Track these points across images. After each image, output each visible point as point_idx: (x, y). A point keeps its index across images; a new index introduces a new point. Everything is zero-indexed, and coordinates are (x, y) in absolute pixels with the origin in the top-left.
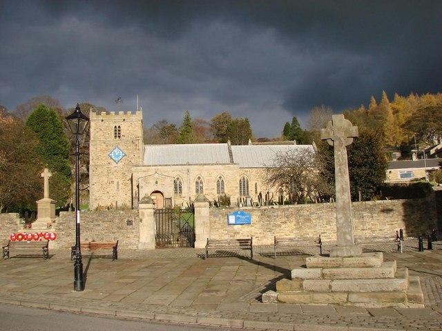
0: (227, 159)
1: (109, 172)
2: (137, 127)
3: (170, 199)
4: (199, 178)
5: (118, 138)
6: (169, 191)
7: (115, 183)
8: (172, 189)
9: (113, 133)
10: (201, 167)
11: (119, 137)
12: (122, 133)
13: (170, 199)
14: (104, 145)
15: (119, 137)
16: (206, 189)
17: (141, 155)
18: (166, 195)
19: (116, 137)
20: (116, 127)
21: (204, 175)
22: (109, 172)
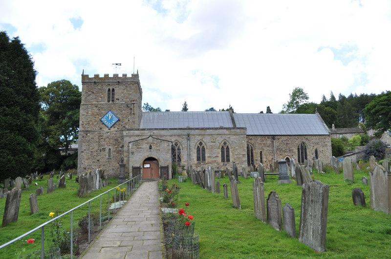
0: (231, 126)
1: (100, 136)
2: (133, 91)
3: (167, 167)
4: (201, 144)
5: (111, 102)
6: (165, 158)
7: (107, 150)
9: (106, 98)
10: (202, 132)
11: (113, 101)
12: (116, 97)
13: (167, 167)
14: (96, 110)
15: (113, 101)
16: (209, 157)
17: (137, 120)
18: (162, 163)
19: (109, 101)
20: (109, 90)
21: (207, 140)
22: (100, 136)
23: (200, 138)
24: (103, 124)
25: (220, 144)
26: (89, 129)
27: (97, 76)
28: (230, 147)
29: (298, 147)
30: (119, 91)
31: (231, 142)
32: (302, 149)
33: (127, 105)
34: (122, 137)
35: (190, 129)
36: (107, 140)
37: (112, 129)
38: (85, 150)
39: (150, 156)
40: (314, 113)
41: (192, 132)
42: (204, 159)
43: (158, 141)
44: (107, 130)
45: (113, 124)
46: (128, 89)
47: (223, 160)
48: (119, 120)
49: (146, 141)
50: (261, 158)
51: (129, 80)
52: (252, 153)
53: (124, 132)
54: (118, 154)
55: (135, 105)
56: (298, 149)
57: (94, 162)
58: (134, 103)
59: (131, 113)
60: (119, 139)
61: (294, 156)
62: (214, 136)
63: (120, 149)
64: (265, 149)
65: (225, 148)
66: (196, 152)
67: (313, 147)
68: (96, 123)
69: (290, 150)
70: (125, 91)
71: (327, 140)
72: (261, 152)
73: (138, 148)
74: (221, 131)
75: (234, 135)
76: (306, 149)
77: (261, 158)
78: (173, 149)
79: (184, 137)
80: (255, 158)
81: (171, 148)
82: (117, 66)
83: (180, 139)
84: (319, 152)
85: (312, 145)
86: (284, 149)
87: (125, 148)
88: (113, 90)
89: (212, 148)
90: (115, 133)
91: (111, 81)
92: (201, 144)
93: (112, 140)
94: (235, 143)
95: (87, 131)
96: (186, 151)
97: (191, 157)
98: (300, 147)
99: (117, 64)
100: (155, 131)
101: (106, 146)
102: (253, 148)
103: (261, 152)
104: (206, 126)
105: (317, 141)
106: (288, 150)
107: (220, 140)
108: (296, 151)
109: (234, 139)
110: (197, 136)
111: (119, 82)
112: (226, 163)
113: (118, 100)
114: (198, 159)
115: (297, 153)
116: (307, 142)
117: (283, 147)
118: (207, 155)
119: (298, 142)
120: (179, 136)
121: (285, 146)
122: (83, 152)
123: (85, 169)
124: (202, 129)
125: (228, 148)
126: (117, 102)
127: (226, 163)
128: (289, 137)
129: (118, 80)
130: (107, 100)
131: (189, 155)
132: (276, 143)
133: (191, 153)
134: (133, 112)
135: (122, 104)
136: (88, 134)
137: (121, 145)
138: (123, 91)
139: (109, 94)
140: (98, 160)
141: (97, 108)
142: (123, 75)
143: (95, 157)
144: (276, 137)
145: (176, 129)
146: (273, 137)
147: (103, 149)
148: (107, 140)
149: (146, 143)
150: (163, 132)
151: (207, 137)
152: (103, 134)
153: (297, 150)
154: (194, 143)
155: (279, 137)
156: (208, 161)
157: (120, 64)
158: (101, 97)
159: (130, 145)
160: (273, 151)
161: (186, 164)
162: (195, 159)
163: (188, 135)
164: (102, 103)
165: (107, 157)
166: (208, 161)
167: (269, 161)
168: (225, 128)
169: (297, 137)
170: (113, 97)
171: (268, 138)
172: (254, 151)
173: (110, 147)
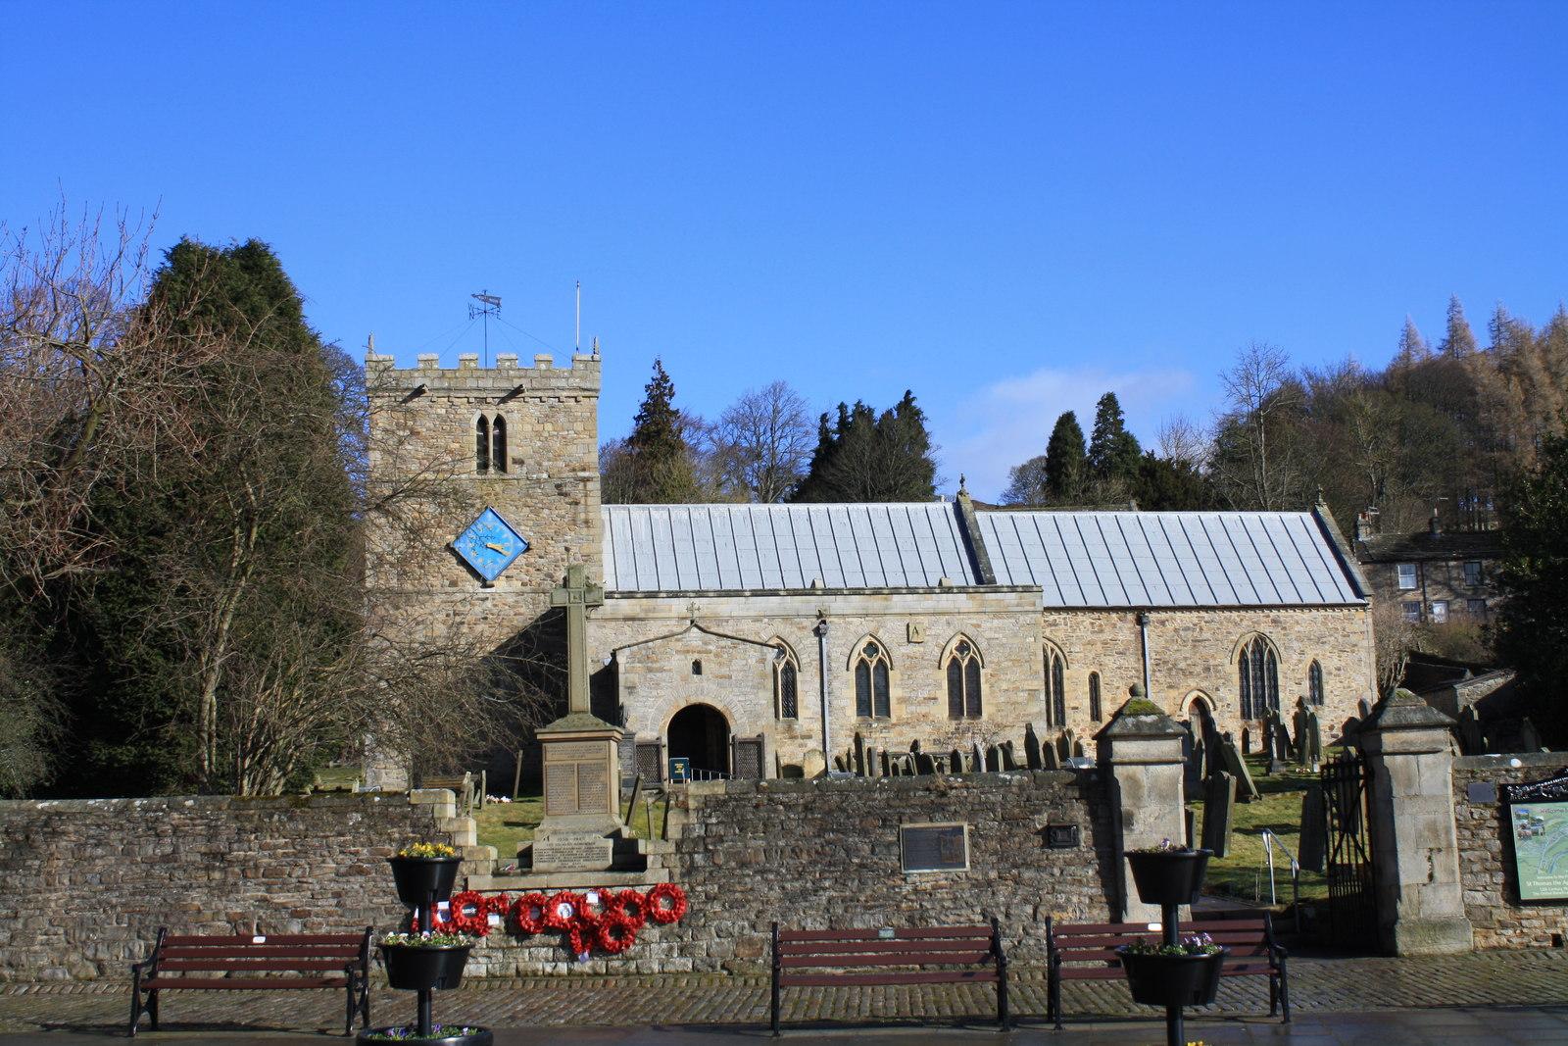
8: (765, 697)
10: (876, 603)
11: (502, 467)
12: (512, 451)
16: (902, 701)
19: (483, 466)
20: (483, 422)
21: (891, 634)
23: (869, 625)
29: (1243, 653)
33: (558, 486)
39: (694, 700)
41: (836, 604)
42: (885, 709)
46: (562, 418)
47: (956, 710)
51: (562, 383)
55: (590, 485)
58: (585, 480)
59: (574, 521)
64: (1110, 662)
67: (1302, 653)
69: (1207, 669)
71: (1358, 626)
72: (1094, 678)
73: (650, 670)
75: (997, 614)
80: (1069, 703)
85: (1295, 645)
86: (1182, 665)
88: (500, 422)
89: (913, 664)
90: (511, 600)
92: (872, 648)
94: (1003, 645)
103: (1094, 678)
105: (1318, 629)
106: (1198, 669)
108: (1233, 670)
112: (965, 721)
113: (521, 462)
114: (863, 707)
115: (1236, 677)
116: (1274, 635)
117: (1182, 655)
118: (895, 693)
119: (1243, 629)
120: (786, 618)
121: (1187, 651)
127: (965, 721)
134: (582, 516)
138: (539, 427)
139: (483, 441)
144: (1153, 616)
145: (774, 593)
149: (677, 652)
154: (845, 643)
155: (1163, 615)
169: (1235, 614)
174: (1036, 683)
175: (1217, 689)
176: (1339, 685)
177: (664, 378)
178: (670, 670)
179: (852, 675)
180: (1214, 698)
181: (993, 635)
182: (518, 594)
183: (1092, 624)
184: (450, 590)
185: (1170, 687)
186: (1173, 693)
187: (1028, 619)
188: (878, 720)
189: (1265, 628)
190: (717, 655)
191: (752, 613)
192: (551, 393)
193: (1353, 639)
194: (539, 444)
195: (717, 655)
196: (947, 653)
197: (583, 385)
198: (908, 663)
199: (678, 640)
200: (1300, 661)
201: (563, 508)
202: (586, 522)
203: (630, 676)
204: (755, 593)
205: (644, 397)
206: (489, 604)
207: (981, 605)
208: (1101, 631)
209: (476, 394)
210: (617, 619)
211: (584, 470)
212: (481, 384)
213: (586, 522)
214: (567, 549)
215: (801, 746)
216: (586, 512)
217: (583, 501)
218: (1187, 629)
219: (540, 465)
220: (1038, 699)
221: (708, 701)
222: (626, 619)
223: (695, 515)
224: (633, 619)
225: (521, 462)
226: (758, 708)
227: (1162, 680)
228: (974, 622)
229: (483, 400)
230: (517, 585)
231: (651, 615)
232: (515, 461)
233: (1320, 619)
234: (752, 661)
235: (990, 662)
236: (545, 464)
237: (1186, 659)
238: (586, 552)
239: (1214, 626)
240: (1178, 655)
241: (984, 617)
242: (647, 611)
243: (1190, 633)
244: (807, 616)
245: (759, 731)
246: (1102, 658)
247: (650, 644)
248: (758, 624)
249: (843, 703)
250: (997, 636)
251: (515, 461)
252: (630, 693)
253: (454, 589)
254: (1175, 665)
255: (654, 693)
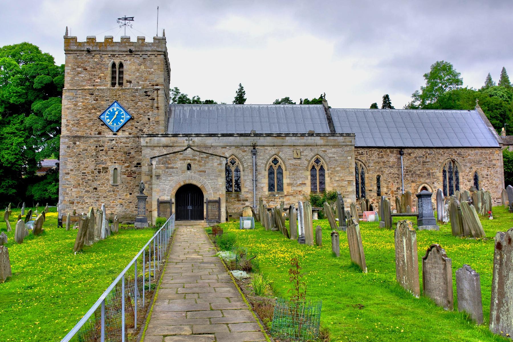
0: (327, 130)
1: (99, 148)
2: (155, 67)
3: (218, 202)
4: (275, 161)
7: (111, 171)
8: (222, 181)
11: (121, 84)
12: (126, 77)
14: (91, 100)
15: (121, 84)
16: (289, 184)
19: (113, 84)
20: (114, 65)
21: (286, 155)
23: (273, 151)
24: (104, 124)
25: (309, 161)
26: (79, 134)
27: (91, 40)
28: (325, 167)
30: (131, 67)
31: (327, 160)
32: (450, 172)
33: (146, 92)
34: (139, 150)
35: (256, 135)
36: (111, 152)
37: (120, 134)
38: (72, 170)
39: (187, 182)
40: (472, 107)
41: (261, 141)
42: (281, 189)
43: (202, 156)
44: (110, 135)
45: (120, 125)
46: (148, 63)
48: (132, 119)
49: (181, 157)
50: (379, 187)
51: (149, 49)
52: (363, 179)
53: (142, 140)
54: (130, 178)
55: (159, 92)
56: (444, 171)
57: (88, 192)
58: (158, 90)
60: (132, 152)
61: (436, 184)
62: (298, 148)
63: (134, 169)
64: (387, 171)
65: (318, 168)
66: (267, 176)
67: (471, 168)
68: (91, 123)
69: (429, 174)
70: (143, 67)
71: (496, 157)
73: (167, 168)
74: (310, 140)
75: (334, 146)
76: (457, 172)
77: (379, 187)
78: (228, 171)
79: (246, 149)
80: (367, 187)
81: (224, 168)
82: (127, 21)
83: (239, 153)
84: (480, 178)
85: (468, 164)
86: (418, 172)
87: (145, 168)
88: (121, 65)
90: (124, 140)
91: (117, 48)
92: (275, 161)
93: (119, 153)
94: (336, 160)
95: (76, 137)
96: (251, 175)
97: (259, 185)
98: (447, 169)
99: (126, 19)
100: (196, 139)
101: (109, 164)
102: (365, 170)
104: (284, 130)
105: (478, 158)
106: (425, 174)
107: (309, 154)
108: (440, 175)
109: (334, 153)
110: (269, 148)
111: (131, 51)
113: (130, 82)
114: (271, 188)
115: (441, 179)
116: (459, 159)
117: (417, 168)
119: (444, 159)
120: (237, 147)
121: (420, 167)
122: (68, 174)
123: (73, 203)
124: (279, 135)
125: (322, 169)
126: (129, 86)
128: (428, 150)
129: (129, 48)
130: (109, 83)
131: (255, 181)
132: (405, 161)
133: (259, 176)
134: (156, 105)
135: (137, 90)
136: (78, 143)
137: (135, 163)
139: (114, 72)
140: (96, 189)
141: (93, 97)
142: (139, 39)
143: (89, 182)
144: (405, 151)
145: (231, 135)
146: (401, 150)
147: (104, 168)
148: (111, 152)
149: (181, 160)
150: (210, 141)
151: (286, 150)
152: (104, 142)
153: (441, 174)
155: (410, 151)
156: (288, 192)
157: (132, 19)
158: (100, 78)
159: (154, 163)
160: (399, 176)
161: (249, 195)
162: (266, 189)
163: (254, 146)
164: (101, 88)
165: (111, 182)
166: (288, 192)
167: (392, 192)
168: (318, 135)
169: (441, 151)
170: (121, 78)
171: (392, 152)
172: (366, 175)
173: (117, 165)
174: (351, 177)
175: (433, 183)
176: (487, 182)
177: (242, 88)
178: (177, 168)
179: (267, 173)
180: (432, 187)
181: (331, 155)
182: (127, 138)
183: (378, 154)
184: (98, 136)
185: (412, 182)
186: (414, 185)
187: (348, 149)
188: (278, 193)
189: (455, 157)
190: (199, 161)
191: (221, 144)
192: (143, 53)
193: (494, 162)
194: (138, 74)
195: (199, 161)
196: (311, 163)
197: (158, 50)
198: (292, 168)
199: (181, 154)
200: (470, 172)
201: (147, 102)
202: (158, 108)
203: (158, 170)
204: (223, 135)
205: (236, 95)
206: (114, 142)
207: (327, 142)
208: (383, 157)
209: (111, 53)
210: (159, 147)
211: (157, 85)
212: (114, 48)
213: (158, 108)
214: (149, 119)
215: (243, 204)
216: (158, 103)
217: (156, 98)
218: (420, 157)
219: (138, 83)
220: (353, 185)
221: (194, 182)
222: (163, 147)
223: (211, 108)
224: (167, 146)
225: (130, 82)
226: (218, 186)
227: (409, 179)
228: (323, 149)
229: (114, 56)
230: (126, 134)
231: (175, 145)
232: (128, 82)
233: (479, 153)
234: (215, 164)
235: (331, 168)
236: (140, 83)
237: (419, 170)
238: (157, 120)
239: (431, 156)
240: (416, 168)
241: (328, 147)
242: (174, 143)
243: (421, 160)
244: (247, 146)
245: (218, 197)
246: (383, 169)
247: (168, 156)
248: (224, 149)
249: (262, 185)
250: (334, 156)
251: (128, 82)
252: (158, 179)
253: (100, 136)
254: (414, 172)
255: (169, 179)
